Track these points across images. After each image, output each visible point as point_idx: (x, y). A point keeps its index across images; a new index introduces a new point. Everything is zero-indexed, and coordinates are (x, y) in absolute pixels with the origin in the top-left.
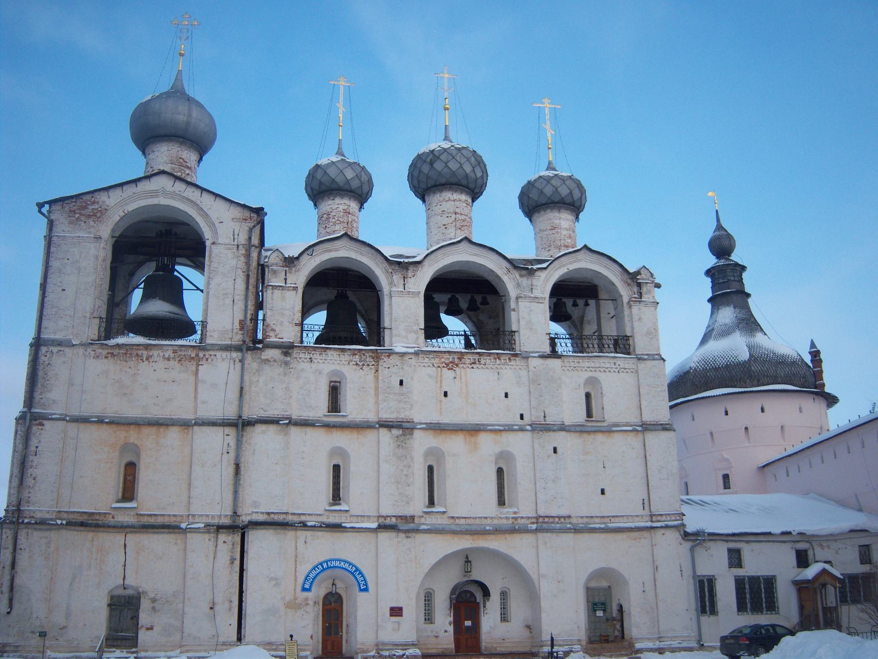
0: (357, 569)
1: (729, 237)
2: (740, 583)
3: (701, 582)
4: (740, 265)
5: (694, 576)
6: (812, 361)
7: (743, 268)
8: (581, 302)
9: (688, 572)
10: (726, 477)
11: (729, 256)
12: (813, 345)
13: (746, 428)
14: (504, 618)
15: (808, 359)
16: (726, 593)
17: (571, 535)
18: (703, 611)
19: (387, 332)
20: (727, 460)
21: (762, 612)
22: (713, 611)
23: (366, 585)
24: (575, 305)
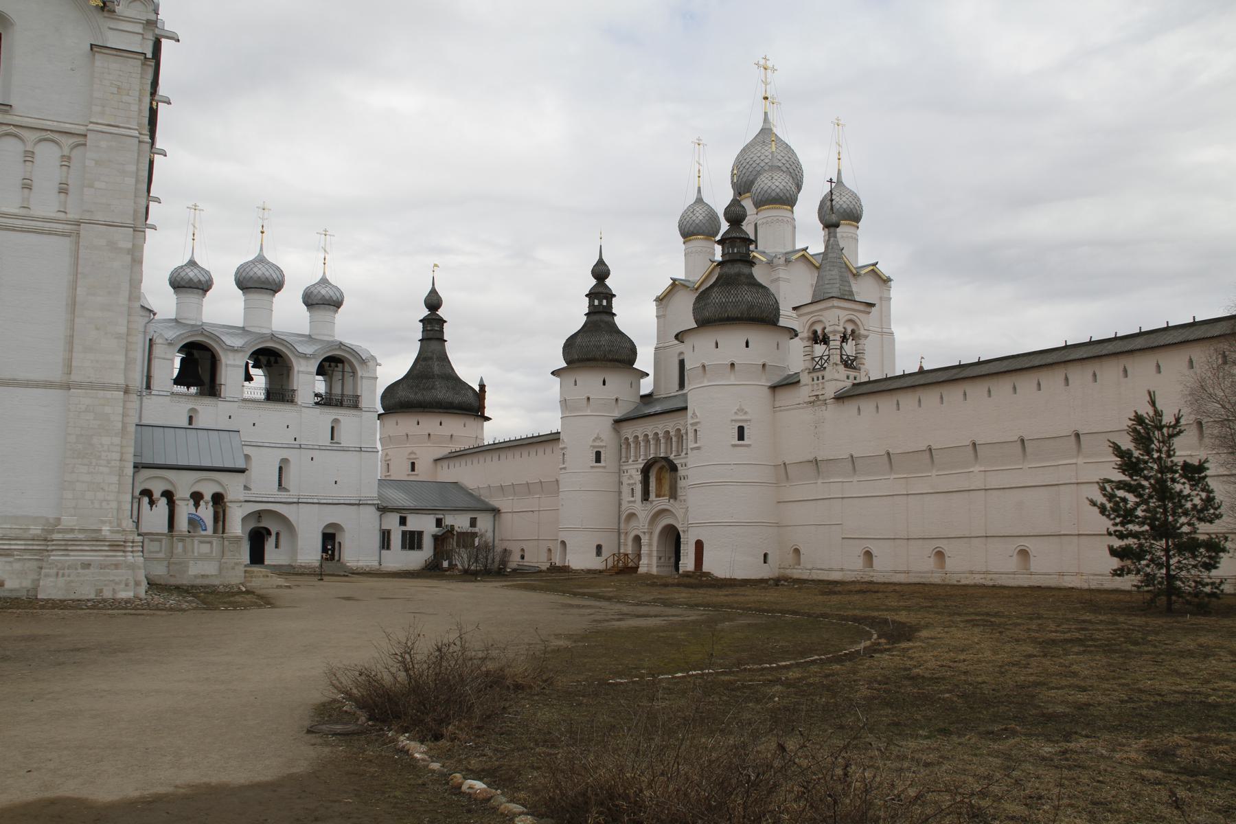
0: (201, 519)
2: (404, 533)
3: (384, 533)
5: (380, 530)
7: (445, 322)
8: (333, 364)
9: (378, 527)
10: (413, 464)
13: (429, 434)
14: (277, 546)
15: (477, 388)
16: (396, 539)
17: (317, 505)
18: (383, 548)
19: (223, 386)
20: (415, 454)
21: (414, 549)
22: (388, 548)
23: (206, 527)
24: (330, 366)
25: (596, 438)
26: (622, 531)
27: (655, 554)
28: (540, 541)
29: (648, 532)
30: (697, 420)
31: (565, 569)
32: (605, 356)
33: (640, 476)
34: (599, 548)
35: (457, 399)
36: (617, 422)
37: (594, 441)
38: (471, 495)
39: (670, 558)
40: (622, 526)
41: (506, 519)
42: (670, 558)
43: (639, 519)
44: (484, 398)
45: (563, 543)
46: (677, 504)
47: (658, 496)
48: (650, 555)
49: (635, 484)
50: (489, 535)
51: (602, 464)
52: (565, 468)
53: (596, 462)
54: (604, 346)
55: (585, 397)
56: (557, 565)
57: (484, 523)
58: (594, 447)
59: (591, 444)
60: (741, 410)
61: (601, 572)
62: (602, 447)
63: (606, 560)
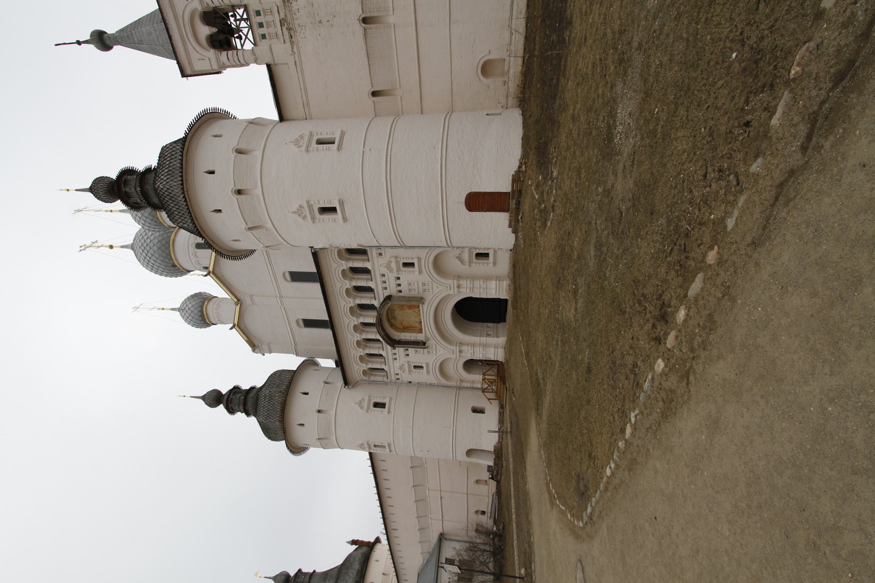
1: (281, 574)
4: (297, 572)
6: (356, 545)
7: (300, 570)
11: (291, 577)
12: (348, 542)
15: (355, 547)
25: (359, 406)
26: (458, 384)
27: (484, 339)
28: (469, 492)
29: (460, 347)
30: (305, 205)
31: (498, 452)
32: (281, 392)
33: (400, 349)
34: (475, 410)
35: (357, 566)
36: (346, 382)
37: (362, 408)
38: (428, 561)
39: (488, 327)
40: (453, 384)
41: (448, 527)
42: (488, 327)
43: (379, 16)
44: (362, 542)
45: (470, 452)
46: (428, 297)
47: (421, 331)
48: (485, 346)
49: (408, 362)
50: (458, 546)
51: (386, 401)
52: (389, 445)
53: (385, 408)
54: (270, 391)
55: (316, 415)
56: (491, 464)
57: (449, 551)
58: (368, 409)
59: (364, 411)
60: (297, 143)
61: (502, 407)
62: (370, 400)
63: (489, 399)
